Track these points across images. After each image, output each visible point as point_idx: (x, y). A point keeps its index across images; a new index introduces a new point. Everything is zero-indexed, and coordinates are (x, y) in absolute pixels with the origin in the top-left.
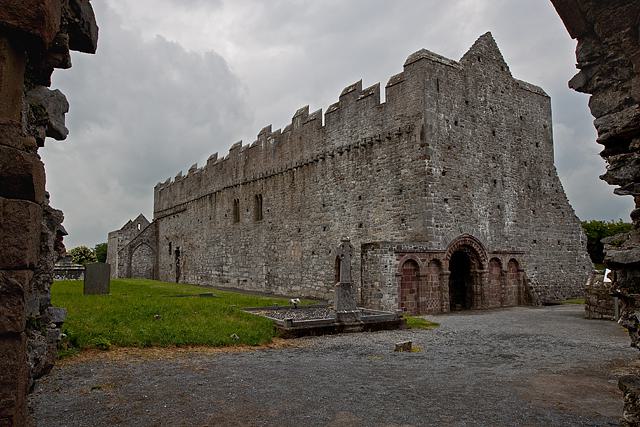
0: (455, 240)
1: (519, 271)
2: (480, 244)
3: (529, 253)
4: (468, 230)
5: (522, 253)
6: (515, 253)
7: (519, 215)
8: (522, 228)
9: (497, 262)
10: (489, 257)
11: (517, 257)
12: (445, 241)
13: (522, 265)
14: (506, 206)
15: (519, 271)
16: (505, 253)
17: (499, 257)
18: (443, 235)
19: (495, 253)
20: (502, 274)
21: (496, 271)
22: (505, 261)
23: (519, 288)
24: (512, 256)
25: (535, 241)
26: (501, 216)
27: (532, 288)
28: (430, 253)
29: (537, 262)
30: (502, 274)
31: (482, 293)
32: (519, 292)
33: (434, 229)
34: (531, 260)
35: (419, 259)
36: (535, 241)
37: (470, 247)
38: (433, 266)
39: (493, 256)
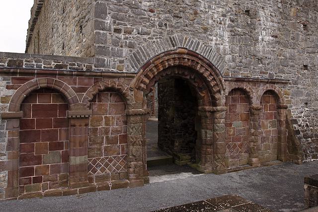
0: (158, 58)
1: (279, 107)
2: (210, 65)
3: (296, 83)
4: (186, 41)
5: (285, 83)
6: (273, 82)
7: (283, 27)
8: (286, 46)
9: (241, 93)
10: (228, 87)
11: (277, 88)
12: (135, 58)
13: (284, 100)
14: (261, 13)
15: (279, 107)
16: (256, 82)
17: (246, 86)
18: (131, 46)
19: (238, 80)
20: (251, 113)
21: (241, 108)
22: (257, 93)
23: (279, 132)
24: (269, 87)
25: (306, 67)
26: (252, 27)
27: (298, 132)
28: (98, 77)
29: (308, 95)
30: (251, 113)
31: (213, 143)
32: (279, 139)
33: (110, 37)
34: (298, 93)
35: (69, 88)
36: (306, 67)
37: (191, 70)
38: (109, 102)
39: (234, 85)
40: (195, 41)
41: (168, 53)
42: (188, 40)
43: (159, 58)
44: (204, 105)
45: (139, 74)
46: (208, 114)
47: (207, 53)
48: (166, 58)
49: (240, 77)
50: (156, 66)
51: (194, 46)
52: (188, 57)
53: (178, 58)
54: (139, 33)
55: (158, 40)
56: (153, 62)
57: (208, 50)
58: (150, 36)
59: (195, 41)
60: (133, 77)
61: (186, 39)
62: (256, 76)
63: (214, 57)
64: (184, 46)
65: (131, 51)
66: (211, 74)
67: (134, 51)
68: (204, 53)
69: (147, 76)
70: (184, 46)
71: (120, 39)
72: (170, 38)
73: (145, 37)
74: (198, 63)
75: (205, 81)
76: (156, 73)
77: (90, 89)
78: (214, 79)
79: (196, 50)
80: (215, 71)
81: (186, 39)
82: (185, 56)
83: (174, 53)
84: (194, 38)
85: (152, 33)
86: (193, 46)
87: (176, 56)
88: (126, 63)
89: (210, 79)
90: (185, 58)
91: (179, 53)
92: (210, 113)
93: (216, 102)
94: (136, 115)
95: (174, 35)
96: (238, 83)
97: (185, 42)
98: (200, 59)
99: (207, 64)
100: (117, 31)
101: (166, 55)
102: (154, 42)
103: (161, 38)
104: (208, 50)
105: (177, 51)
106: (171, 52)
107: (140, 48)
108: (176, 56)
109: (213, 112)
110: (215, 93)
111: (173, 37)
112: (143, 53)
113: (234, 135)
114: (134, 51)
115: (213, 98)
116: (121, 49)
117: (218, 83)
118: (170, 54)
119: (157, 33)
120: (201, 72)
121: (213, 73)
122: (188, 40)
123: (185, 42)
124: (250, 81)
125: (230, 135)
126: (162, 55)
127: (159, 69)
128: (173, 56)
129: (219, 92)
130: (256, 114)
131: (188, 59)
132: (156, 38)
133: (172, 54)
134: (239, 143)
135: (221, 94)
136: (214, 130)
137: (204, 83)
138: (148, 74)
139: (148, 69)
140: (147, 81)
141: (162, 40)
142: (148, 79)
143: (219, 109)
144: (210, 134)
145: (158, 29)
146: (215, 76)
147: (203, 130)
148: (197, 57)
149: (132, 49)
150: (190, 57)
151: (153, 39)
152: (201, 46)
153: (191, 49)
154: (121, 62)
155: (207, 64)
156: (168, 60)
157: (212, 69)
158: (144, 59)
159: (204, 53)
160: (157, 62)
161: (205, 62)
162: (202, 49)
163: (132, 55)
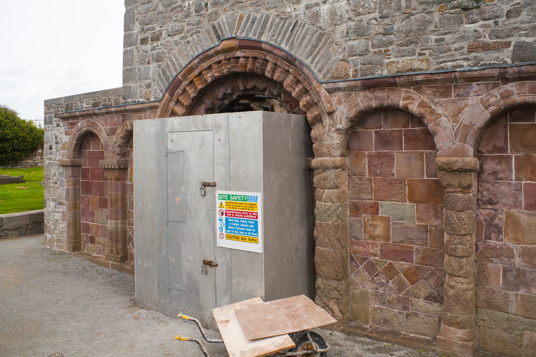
18: (158, 59)
40: (259, 16)
41: (205, 56)
42: (244, 19)
47: (285, 34)
48: (205, 65)
49: (385, 73)
51: (257, 28)
52: (242, 54)
53: (226, 59)
54: (169, 36)
55: (195, 36)
56: (185, 77)
57: (289, 26)
58: (182, 35)
59: (259, 16)
60: (157, 107)
61: (241, 18)
62: (450, 64)
63: (303, 38)
67: (163, 65)
68: (279, 35)
69: (178, 102)
71: (146, 52)
72: (214, 27)
73: (177, 38)
74: (267, 61)
77: (119, 131)
79: (261, 34)
81: (241, 18)
82: (239, 54)
83: (218, 53)
84: (257, 11)
85: (186, 28)
86: (254, 27)
87: (221, 57)
88: (154, 86)
90: (238, 58)
91: (225, 51)
95: (219, 20)
96: (380, 94)
97: (239, 25)
100: (144, 41)
101: (202, 61)
102: (188, 42)
103: (199, 32)
104: (289, 26)
105: (219, 48)
106: (210, 53)
107: (171, 58)
108: (221, 57)
111: (219, 24)
112: (174, 65)
113: (387, 238)
118: (209, 57)
119: (193, 25)
122: (244, 19)
123: (239, 25)
124: (417, 83)
125: (373, 237)
126: (196, 61)
128: (216, 59)
130: (449, 185)
131: (247, 58)
132: (191, 36)
134: (406, 265)
141: (200, 35)
145: (194, 18)
148: (261, 49)
149: (160, 63)
150: (248, 53)
151: (187, 37)
152: (272, 23)
153: (251, 36)
154: (148, 86)
156: (210, 67)
159: (279, 35)
160: (191, 76)
162: (273, 27)
163: (161, 72)
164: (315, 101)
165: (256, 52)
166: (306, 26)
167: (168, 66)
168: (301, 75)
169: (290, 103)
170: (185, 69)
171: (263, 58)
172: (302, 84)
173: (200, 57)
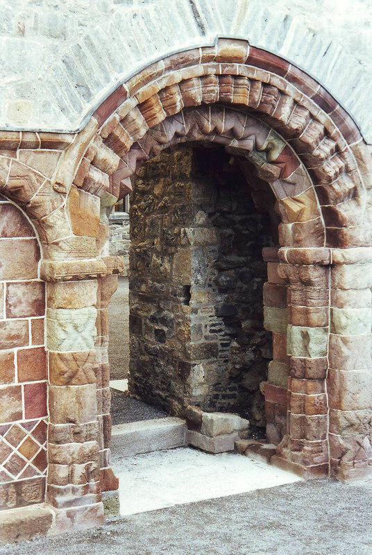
2: (327, 103)
43: (151, 78)
44: (297, 242)
45: (84, 138)
46: (314, 274)
47: (314, 58)
48: (178, 75)
50: (143, 107)
53: (217, 75)
64: (237, 30)
65: (55, 50)
66: (327, 134)
69: (111, 141)
70: (237, 30)
75: (305, 161)
76: (143, 132)
78: (337, 151)
80: (340, 122)
82: (239, 69)
89: (323, 149)
90: (240, 77)
91: (223, 59)
92: (321, 271)
93: (340, 232)
94: (76, 278)
98: (293, 79)
99: (317, 98)
101: (176, 65)
105: (216, 52)
109: (331, 267)
110: (338, 198)
114: (66, 49)
115: (332, 216)
116: (18, 39)
117: (351, 167)
118: (187, 63)
120: (295, 126)
121: (335, 130)
127: (153, 117)
129: (354, 194)
133: (196, 62)
135: (359, 205)
136: (333, 327)
137: (301, 166)
138: (117, 133)
139: (115, 116)
140: (112, 159)
142: (117, 152)
143: (353, 258)
144: (318, 343)
146: (342, 142)
147: (294, 328)
155: (317, 98)
157: (335, 116)
158: (102, 81)
161: (307, 91)
164: (351, 169)
165: (272, 76)
166: (343, 53)
167: (82, 58)
168: (335, 128)
169: (282, 165)
170: (141, 75)
171: (282, 89)
172: (333, 139)
173: (175, 58)
